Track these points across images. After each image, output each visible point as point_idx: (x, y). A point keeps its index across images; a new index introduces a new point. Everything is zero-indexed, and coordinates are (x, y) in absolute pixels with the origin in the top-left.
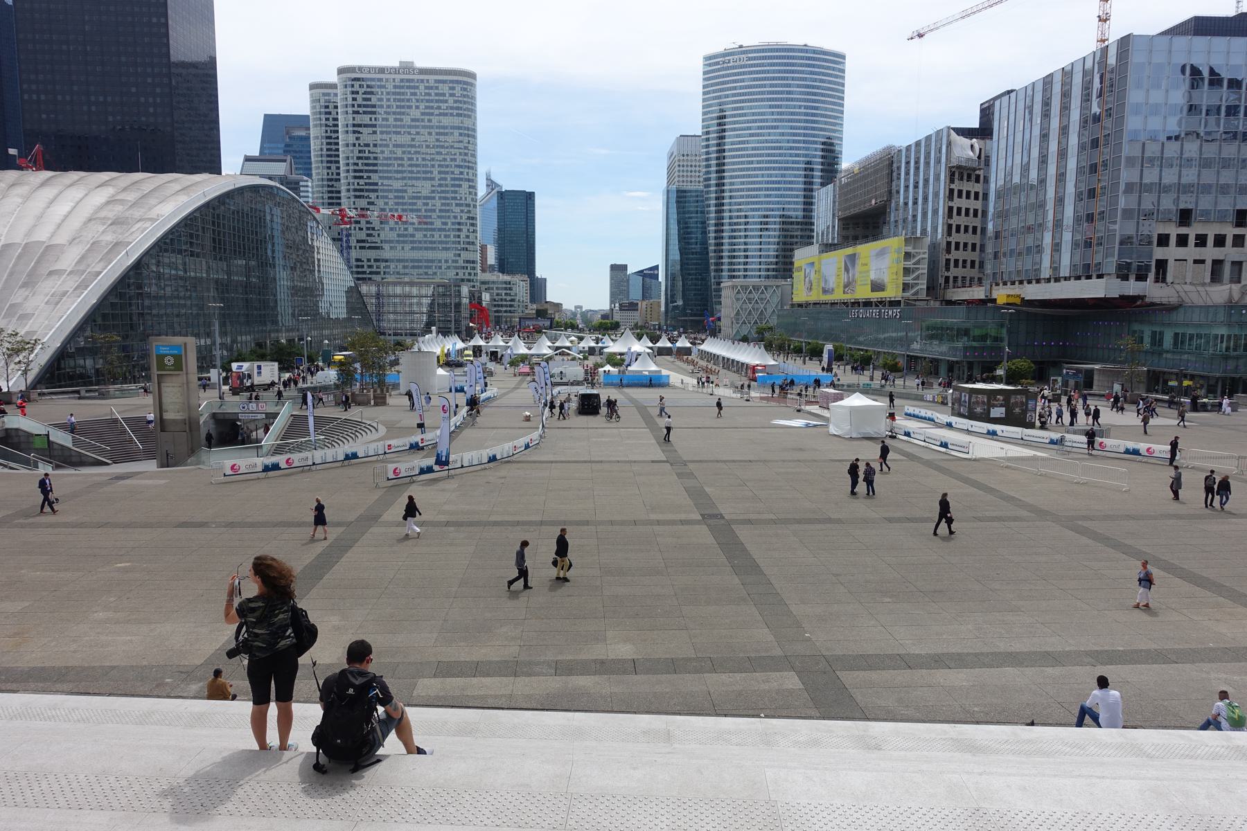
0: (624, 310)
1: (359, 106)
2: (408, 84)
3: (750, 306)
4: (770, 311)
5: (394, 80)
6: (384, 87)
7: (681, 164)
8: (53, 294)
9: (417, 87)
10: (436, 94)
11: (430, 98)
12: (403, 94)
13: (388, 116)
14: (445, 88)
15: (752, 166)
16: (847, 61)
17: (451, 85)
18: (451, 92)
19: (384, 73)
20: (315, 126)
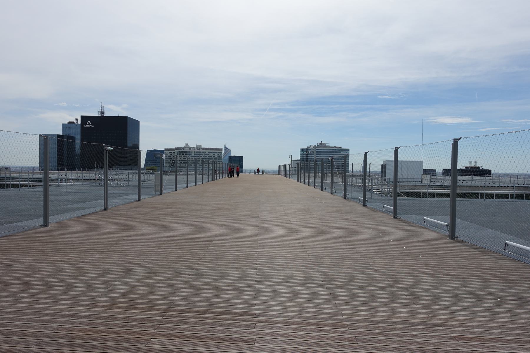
1: (182, 161)
2: (199, 153)
5: (194, 152)
6: (191, 154)
9: (202, 154)
10: (209, 157)
11: (207, 158)
12: (197, 157)
13: (192, 164)
14: (211, 155)
17: (214, 154)
18: (214, 156)
20: (166, 163)
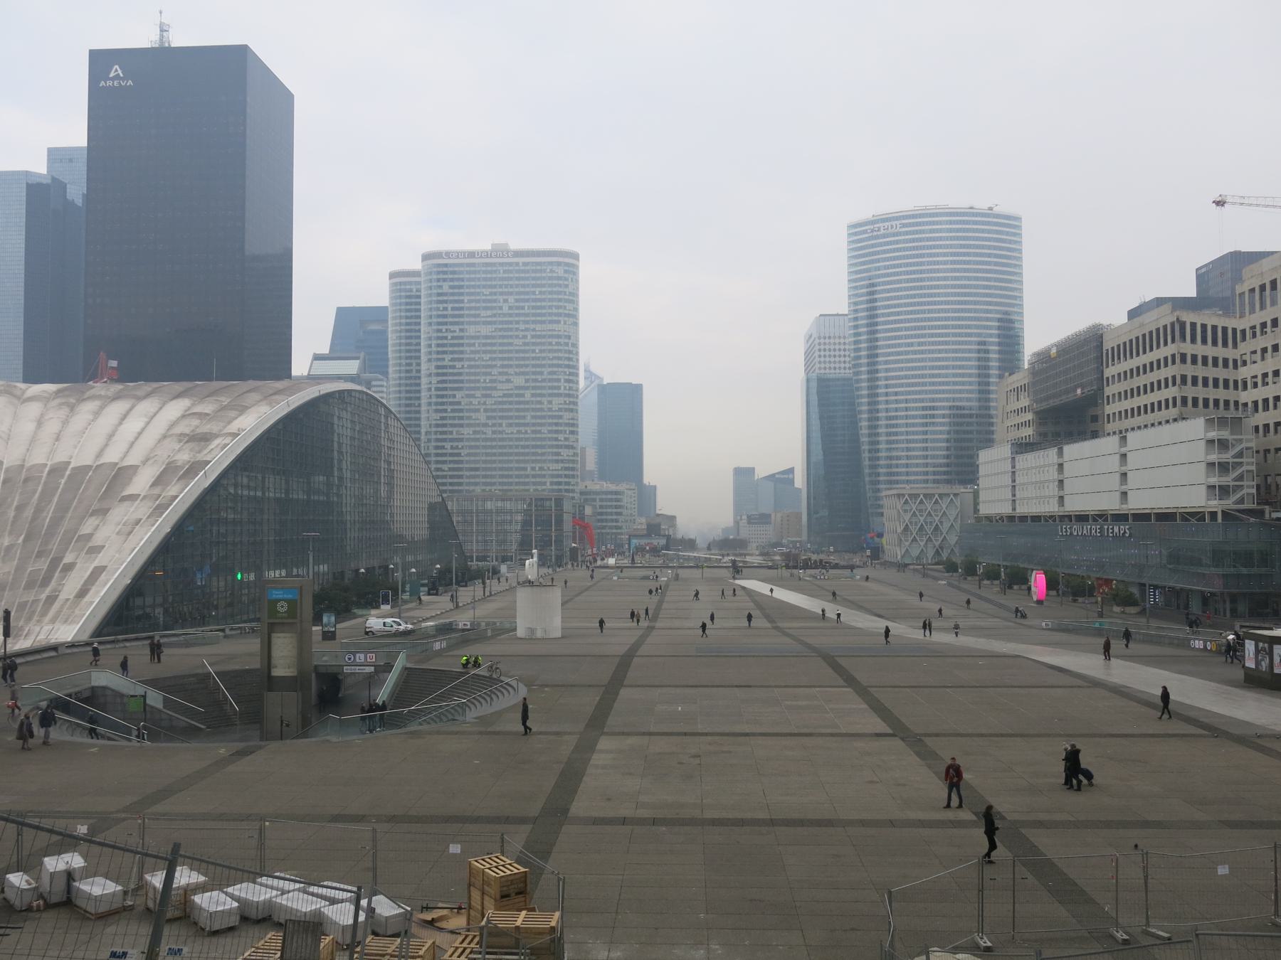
0: (753, 523)
3: (922, 519)
4: (946, 526)
7: (822, 347)
8: (125, 522)
15: (912, 349)
16: (1025, 224)
19: (474, 257)
